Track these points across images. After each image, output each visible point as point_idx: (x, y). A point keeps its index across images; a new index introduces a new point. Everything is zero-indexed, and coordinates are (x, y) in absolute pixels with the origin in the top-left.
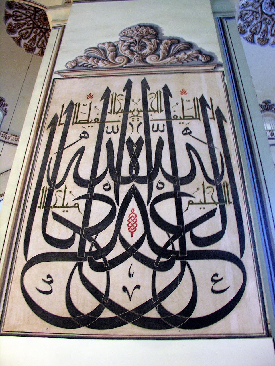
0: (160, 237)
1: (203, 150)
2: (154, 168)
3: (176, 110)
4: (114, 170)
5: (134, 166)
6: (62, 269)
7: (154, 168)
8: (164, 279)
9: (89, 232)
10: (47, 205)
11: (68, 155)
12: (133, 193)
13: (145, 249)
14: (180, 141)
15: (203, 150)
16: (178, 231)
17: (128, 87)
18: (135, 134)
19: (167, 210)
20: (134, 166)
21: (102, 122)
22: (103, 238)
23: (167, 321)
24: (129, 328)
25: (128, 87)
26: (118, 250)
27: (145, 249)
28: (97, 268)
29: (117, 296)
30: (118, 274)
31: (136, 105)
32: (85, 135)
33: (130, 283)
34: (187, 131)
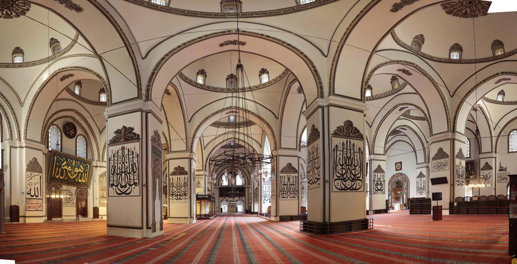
0: (352, 176)
1: (359, 160)
2: (352, 163)
3: (355, 151)
4: (346, 163)
5: (349, 163)
6: (339, 181)
7: (352, 163)
8: (353, 183)
9: (343, 175)
10: (336, 170)
11: (338, 158)
12: (349, 168)
13: (350, 178)
14: (356, 158)
15: (359, 160)
16: (355, 176)
17: (347, 142)
18: (349, 155)
19: (353, 172)
20: (349, 163)
21: (343, 151)
22: (345, 176)
23: (353, 189)
24: (349, 190)
25: (347, 142)
26: (347, 178)
27: (350, 178)
28: (344, 181)
29: (347, 186)
30: (347, 182)
31: (349, 148)
32: (340, 154)
33: (349, 184)
34: (357, 156)
